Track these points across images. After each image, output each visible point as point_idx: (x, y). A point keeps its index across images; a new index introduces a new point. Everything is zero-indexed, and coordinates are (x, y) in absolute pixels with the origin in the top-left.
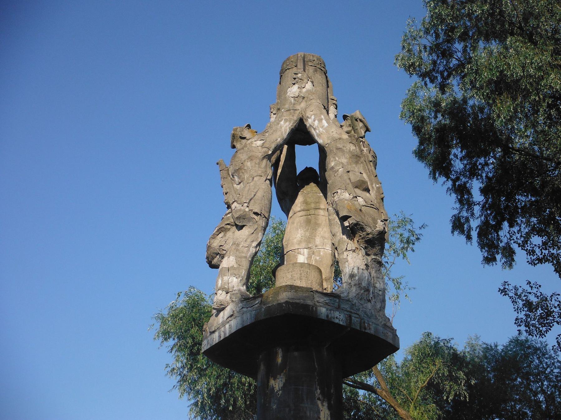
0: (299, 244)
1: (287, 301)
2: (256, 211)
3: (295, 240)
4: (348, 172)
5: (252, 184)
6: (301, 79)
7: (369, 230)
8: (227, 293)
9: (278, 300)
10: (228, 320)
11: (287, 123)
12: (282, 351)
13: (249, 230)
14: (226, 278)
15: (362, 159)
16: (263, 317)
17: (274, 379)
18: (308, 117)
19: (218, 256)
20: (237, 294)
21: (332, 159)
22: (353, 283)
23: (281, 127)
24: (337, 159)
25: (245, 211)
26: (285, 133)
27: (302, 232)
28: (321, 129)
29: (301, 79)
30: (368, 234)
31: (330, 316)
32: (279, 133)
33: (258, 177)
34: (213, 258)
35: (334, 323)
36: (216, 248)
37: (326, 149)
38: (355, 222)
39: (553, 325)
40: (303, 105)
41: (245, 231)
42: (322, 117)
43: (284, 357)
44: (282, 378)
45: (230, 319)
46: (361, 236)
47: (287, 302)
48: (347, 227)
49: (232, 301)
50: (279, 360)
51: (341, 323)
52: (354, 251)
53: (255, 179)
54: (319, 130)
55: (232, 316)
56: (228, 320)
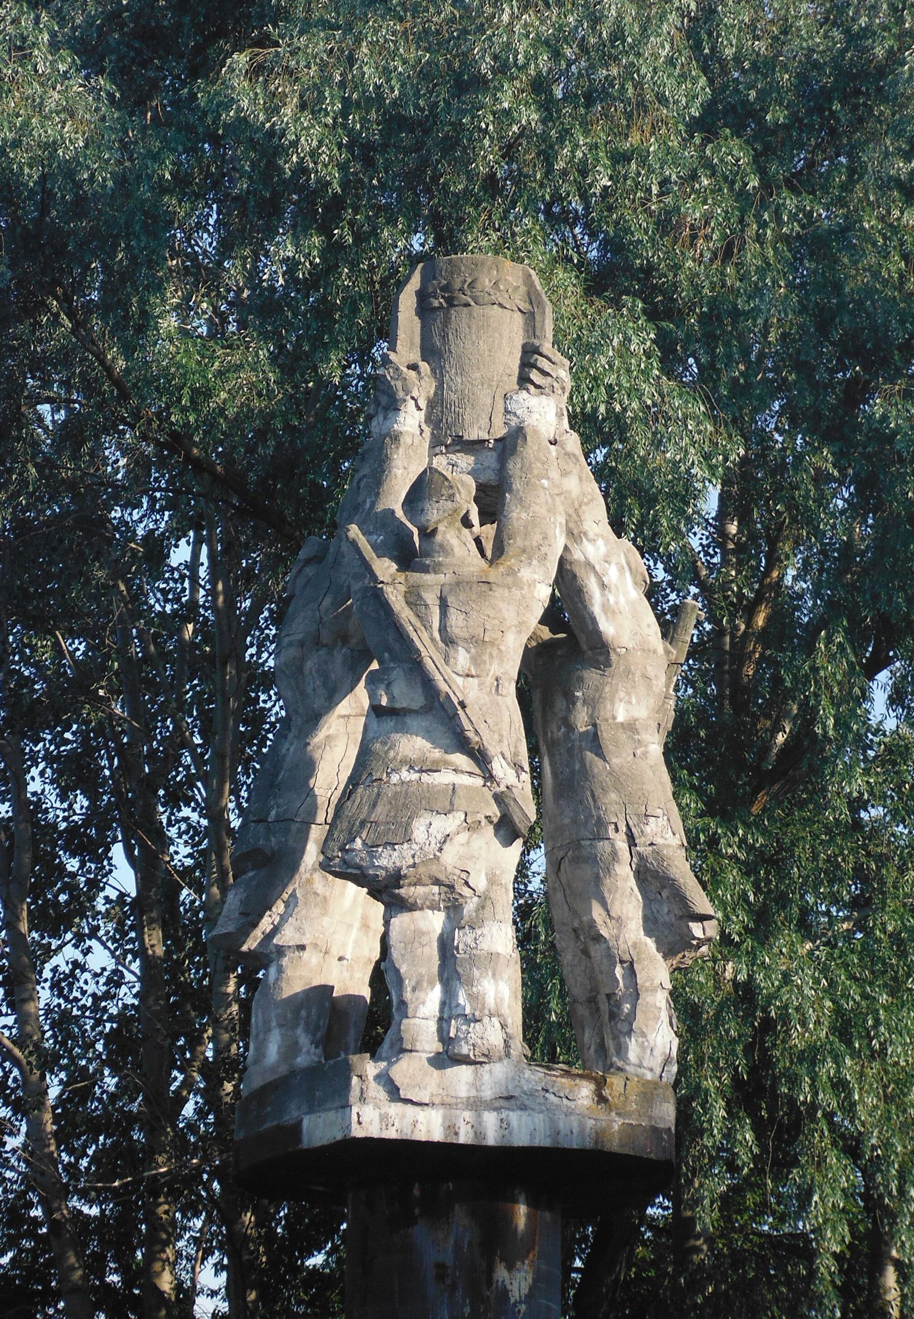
9: (650, 1118)
10: (497, 1104)
16: (614, 1145)
18: (585, 534)
19: (436, 889)
21: (622, 694)
36: (449, 869)
37: (613, 656)
45: (502, 1103)
48: (694, 938)
54: (617, 597)
55: (509, 1098)
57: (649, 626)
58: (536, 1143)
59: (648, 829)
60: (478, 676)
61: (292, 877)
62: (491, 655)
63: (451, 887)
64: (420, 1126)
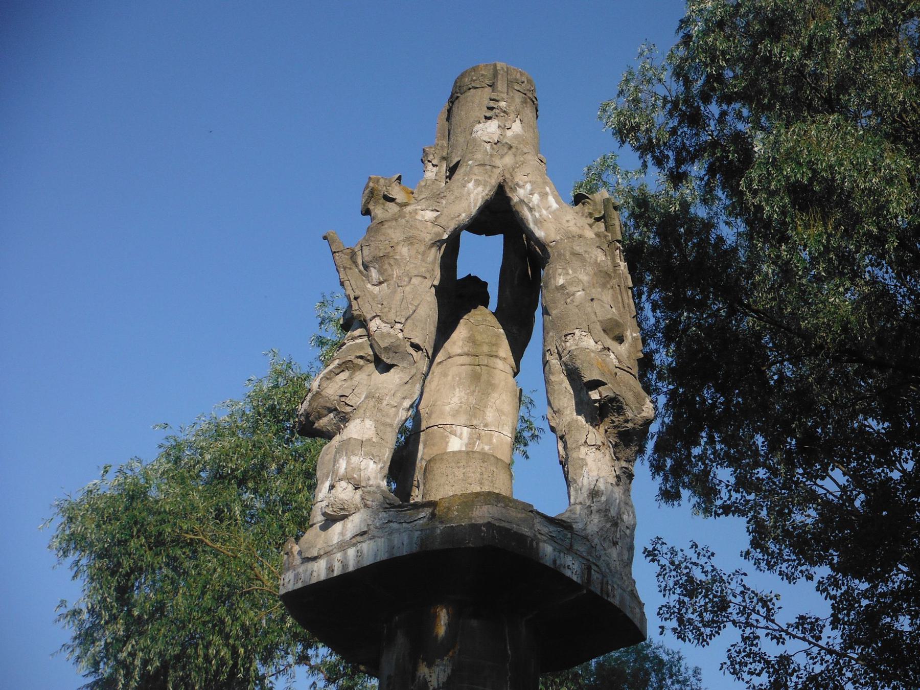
0: (454, 416)
1: (489, 523)
2: (416, 341)
3: (447, 408)
4: (592, 300)
5: (408, 289)
6: (505, 112)
7: (630, 414)
8: (356, 489)
9: (471, 518)
10: (354, 541)
11: (480, 189)
12: (448, 613)
13: (401, 375)
14: (355, 460)
15: (614, 282)
16: (437, 545)
17: (430, 666)
18: (517, 184)
19: (332, 415)
20: (374, 493)
21: (560, 271)
22: (594, 508)
23: (469, 194)
24: (570, 272)
25: (398, 339)
26: (475, 205)
27: (463, 394)
28: (544, 212)
29: (505, 112)
30: (627, 421)
31: (558, 562)
32: (464, 204)
33: (419, 279)
34: (320, 417)
35: (564, 575)
36: (332, 398)
37: (549, 250)
38: (612, 395)
39: (724, 626)
40: (508, 160)
41: (394, 377)
42: (548, 189)
43: (449, 626)
44: (445, 665)
45: (359, 538)
46: (613, 422)
47: (489, 525)
48: (595, 401)
49: (366, 506)
50: (441, 630)
51: (575, 578)
52: (598, 448)
53: (414, 280)
54: (540, 212)
55: (364, 533)
56: (354, 541)
57: (568, 221)
58: (378, 559)
59: (568, 344)
60: (385, 281)
61: (414, 470)
62: (390, 264)
63: (336, 409)
64: (315, 574)
